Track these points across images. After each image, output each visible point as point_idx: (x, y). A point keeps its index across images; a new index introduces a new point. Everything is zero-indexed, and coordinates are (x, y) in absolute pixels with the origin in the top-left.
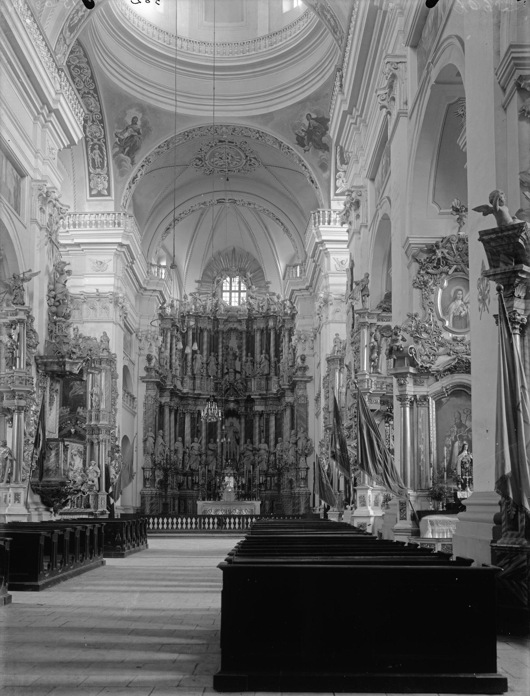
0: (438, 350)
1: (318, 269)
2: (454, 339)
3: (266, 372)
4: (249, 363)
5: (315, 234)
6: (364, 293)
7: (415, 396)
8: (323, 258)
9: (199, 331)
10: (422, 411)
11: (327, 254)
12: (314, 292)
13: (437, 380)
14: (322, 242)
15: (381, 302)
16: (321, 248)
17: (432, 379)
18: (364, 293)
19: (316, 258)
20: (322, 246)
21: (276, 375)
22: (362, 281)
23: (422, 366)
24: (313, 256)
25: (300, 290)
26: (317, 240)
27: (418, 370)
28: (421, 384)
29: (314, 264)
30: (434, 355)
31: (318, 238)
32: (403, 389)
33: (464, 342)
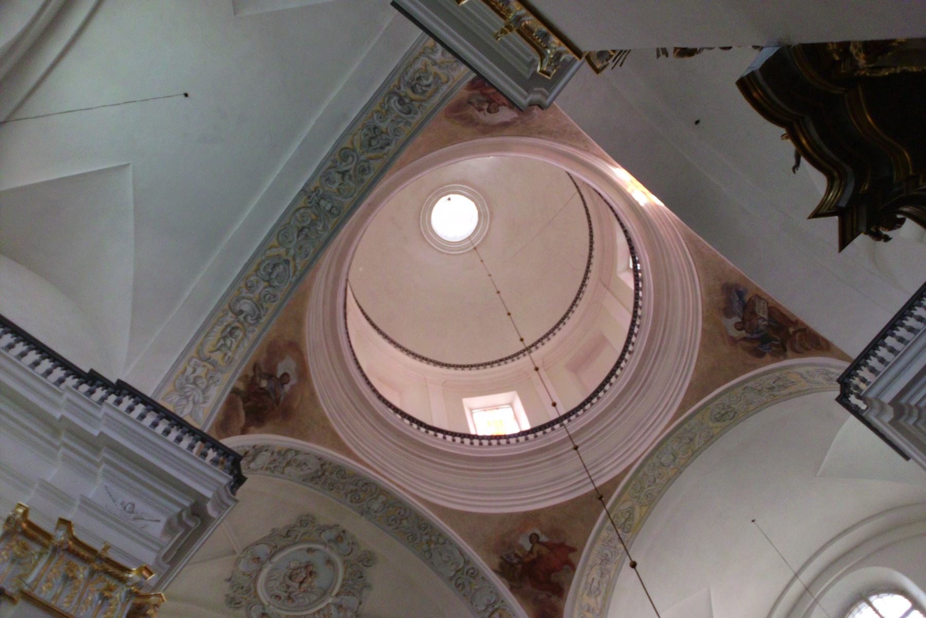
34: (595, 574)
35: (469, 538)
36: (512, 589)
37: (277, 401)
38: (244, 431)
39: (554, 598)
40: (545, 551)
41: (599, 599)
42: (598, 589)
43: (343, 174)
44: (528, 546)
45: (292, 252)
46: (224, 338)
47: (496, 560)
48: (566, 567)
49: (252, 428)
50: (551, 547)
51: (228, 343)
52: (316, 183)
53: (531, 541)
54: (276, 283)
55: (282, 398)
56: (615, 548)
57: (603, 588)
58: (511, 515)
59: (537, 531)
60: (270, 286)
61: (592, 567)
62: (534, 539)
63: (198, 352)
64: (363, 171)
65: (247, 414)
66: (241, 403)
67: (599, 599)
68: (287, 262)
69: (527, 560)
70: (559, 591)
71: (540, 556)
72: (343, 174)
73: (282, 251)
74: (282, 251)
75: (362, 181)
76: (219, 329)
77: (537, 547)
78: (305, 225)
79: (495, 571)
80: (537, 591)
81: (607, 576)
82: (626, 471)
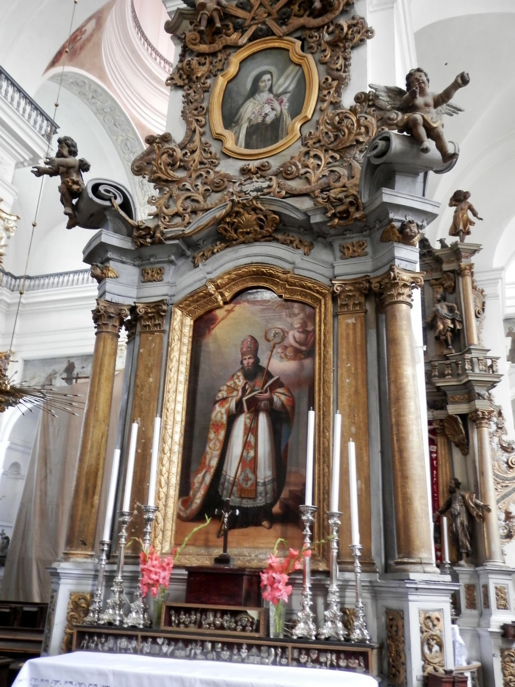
0: (205, 201)
2: (244, 171)
13: (196, 266)
33: (264, 173)
43: (93, 97)
45: (124, 135)
46: (142, 189)
51: (145, 189)
52: (94, 108)
54: (134, 150)
60: (134, 153)
63: (140, 204)
64: (95, 91)
68: (127, 139)
72: (93, 97)
73: (121, 138)
74: (121, 138)
75: (101, 94)
76: (137, 187)
78: (113, 121)
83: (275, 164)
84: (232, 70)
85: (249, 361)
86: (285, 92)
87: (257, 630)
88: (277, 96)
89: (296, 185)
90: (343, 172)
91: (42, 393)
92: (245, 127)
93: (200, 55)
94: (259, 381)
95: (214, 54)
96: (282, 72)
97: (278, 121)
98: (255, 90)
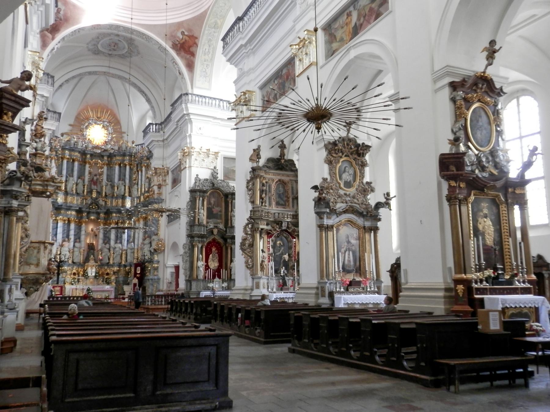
1: (178, 130)
3: (122, 194)
4: (109, 187)
5: (184, 108)
6: (259, 157)
7: (328, 225)
8: (187, 123)
9: (71, 161)
10: (330, 234)
11: (191, 122)
12: (168, 143)
13: (338, 217)
14: (188, 114)
15: (265, 163)
16: (187, 118)
17: (335, 216)
18: (259, 157)
19: (180, 123)
20: (188, 117)
21: (130, 196)
22: (257, 149)
23: (333, 209)
24: (178, 121)
25: (158, 141)
26: (185, 112)
27: (330, 210)
28: (330, 218)
29: (175, 126)
30: (336, 202)
31: (186, 111)
32: (322, 221)
34: (207, 47)
35: (158, 35)
36: (177, 54)
37: (61, 19)
38: (53, 39)
39: (192, 58)
40: (187, 38)
41: (210, 55)
42: (209, 52)
44: (181, 37)
47: (171, 43)
48: (195, 45)
49: (56, 35)
50: (189, 36)
53: (182, 35)
55: (62, 17)
56: (213, 35)
57: (211, 51)
58: (173, 23)
59: (184, 30)
61: (204, 45)
62: (183, 33)
65: (51, 33)
66: (46, 32)
67: (210, 55)
69: (181, 42)
70: (193, 55)
71: (186, 41)
77: (184, 37)
79: (171, 48)
80: (186, 55)
81: (212, 46)
82: (209, 7)
83: (352, 194)
84: (340, 164)
85: (347, 240)
86: (351, 174)
87: (363, 290)
88: (350, 175)
89: (355, 200)
90: (365, 200)
91: (345, 252)
92: (343, 181)
93: (332, 156)
94: (350, 244)
95: (336, 157)
96: (350, 168)
97: (350, 181)
98: (345, 171)
